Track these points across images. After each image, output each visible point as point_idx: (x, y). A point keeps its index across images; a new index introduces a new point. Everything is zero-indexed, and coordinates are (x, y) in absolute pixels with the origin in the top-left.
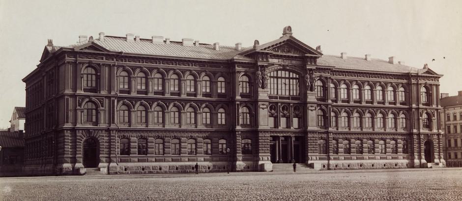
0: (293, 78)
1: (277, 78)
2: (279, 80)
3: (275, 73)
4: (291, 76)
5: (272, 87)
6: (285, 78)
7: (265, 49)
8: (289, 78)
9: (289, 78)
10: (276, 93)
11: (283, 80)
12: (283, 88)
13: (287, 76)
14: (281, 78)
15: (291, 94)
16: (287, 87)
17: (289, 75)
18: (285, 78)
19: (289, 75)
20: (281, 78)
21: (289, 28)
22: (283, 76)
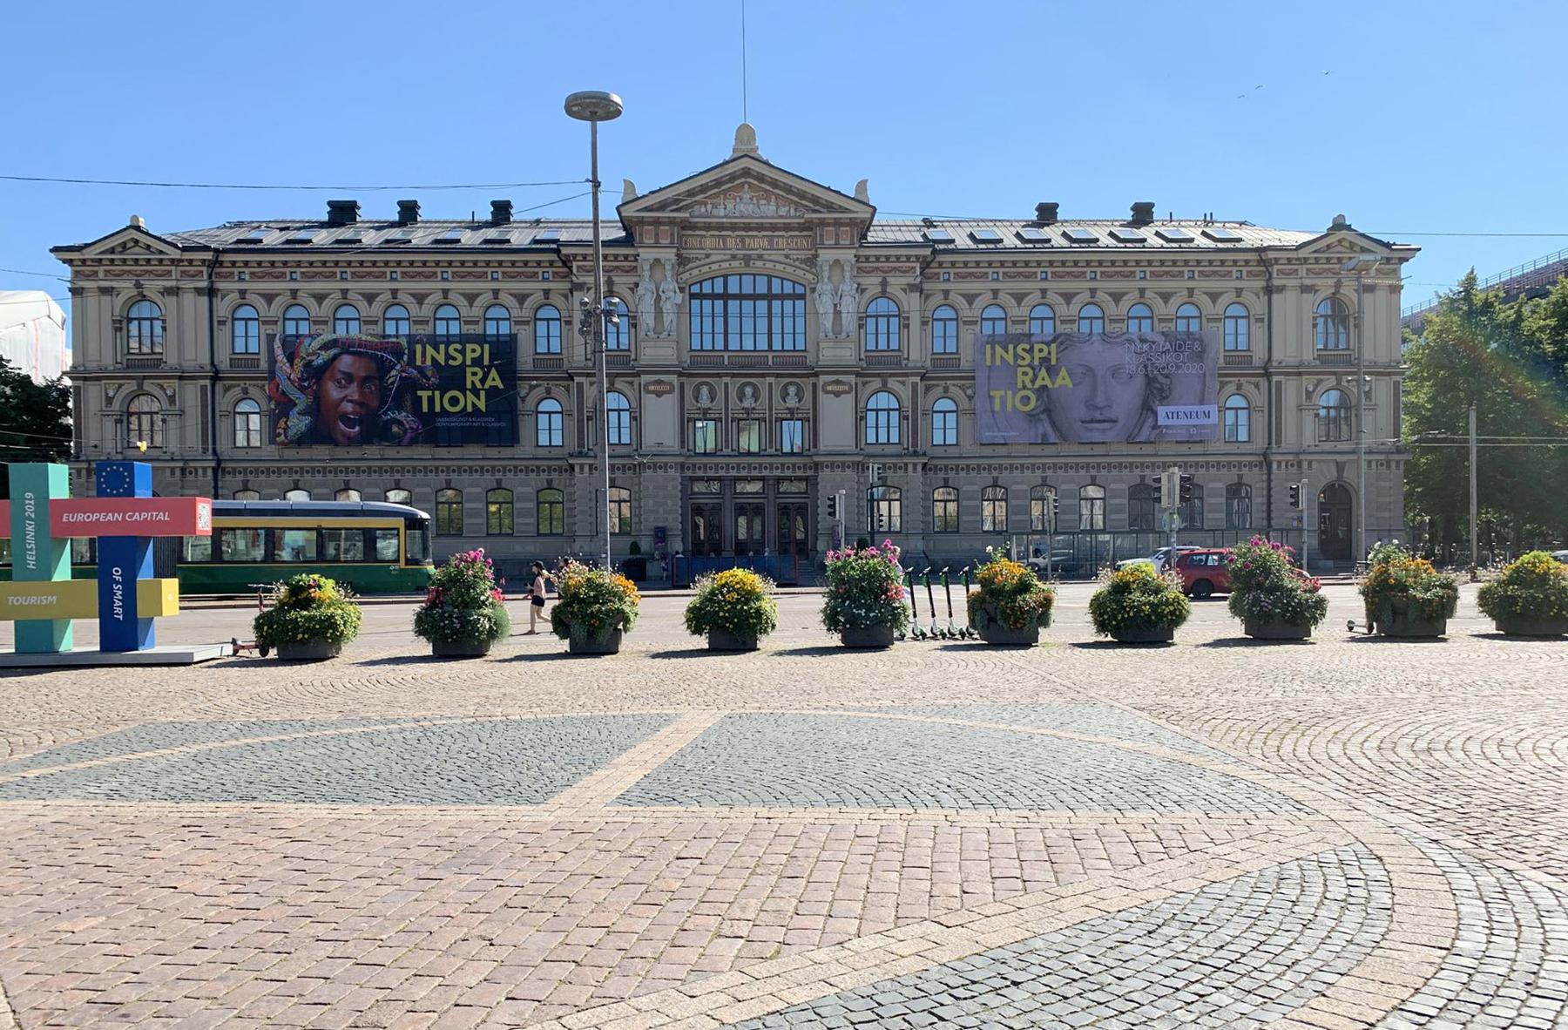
0: (782, 297)
1: (726, 297)
2: (733, 305)
3: (719, 283)
4: (776, 289)
5: (707, 327)
6: (755, 297)
7: (662, 206)
8: (769, 297)
9: (769, 297)
10: (720, 345)
11: (748, 305)
12: (707, 327)
13: (762, 288)
14: (741, 297)
15: (777, 346)
16: (720, 327)
17: (770, 287)
18: (755, 297)
19: (770, 287)
20: (741, 297)
21: (745, 134)
22: (748, 290)
